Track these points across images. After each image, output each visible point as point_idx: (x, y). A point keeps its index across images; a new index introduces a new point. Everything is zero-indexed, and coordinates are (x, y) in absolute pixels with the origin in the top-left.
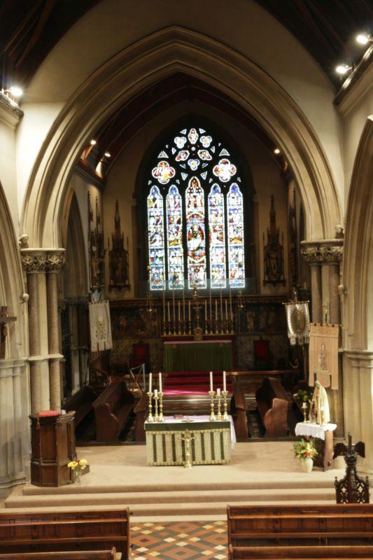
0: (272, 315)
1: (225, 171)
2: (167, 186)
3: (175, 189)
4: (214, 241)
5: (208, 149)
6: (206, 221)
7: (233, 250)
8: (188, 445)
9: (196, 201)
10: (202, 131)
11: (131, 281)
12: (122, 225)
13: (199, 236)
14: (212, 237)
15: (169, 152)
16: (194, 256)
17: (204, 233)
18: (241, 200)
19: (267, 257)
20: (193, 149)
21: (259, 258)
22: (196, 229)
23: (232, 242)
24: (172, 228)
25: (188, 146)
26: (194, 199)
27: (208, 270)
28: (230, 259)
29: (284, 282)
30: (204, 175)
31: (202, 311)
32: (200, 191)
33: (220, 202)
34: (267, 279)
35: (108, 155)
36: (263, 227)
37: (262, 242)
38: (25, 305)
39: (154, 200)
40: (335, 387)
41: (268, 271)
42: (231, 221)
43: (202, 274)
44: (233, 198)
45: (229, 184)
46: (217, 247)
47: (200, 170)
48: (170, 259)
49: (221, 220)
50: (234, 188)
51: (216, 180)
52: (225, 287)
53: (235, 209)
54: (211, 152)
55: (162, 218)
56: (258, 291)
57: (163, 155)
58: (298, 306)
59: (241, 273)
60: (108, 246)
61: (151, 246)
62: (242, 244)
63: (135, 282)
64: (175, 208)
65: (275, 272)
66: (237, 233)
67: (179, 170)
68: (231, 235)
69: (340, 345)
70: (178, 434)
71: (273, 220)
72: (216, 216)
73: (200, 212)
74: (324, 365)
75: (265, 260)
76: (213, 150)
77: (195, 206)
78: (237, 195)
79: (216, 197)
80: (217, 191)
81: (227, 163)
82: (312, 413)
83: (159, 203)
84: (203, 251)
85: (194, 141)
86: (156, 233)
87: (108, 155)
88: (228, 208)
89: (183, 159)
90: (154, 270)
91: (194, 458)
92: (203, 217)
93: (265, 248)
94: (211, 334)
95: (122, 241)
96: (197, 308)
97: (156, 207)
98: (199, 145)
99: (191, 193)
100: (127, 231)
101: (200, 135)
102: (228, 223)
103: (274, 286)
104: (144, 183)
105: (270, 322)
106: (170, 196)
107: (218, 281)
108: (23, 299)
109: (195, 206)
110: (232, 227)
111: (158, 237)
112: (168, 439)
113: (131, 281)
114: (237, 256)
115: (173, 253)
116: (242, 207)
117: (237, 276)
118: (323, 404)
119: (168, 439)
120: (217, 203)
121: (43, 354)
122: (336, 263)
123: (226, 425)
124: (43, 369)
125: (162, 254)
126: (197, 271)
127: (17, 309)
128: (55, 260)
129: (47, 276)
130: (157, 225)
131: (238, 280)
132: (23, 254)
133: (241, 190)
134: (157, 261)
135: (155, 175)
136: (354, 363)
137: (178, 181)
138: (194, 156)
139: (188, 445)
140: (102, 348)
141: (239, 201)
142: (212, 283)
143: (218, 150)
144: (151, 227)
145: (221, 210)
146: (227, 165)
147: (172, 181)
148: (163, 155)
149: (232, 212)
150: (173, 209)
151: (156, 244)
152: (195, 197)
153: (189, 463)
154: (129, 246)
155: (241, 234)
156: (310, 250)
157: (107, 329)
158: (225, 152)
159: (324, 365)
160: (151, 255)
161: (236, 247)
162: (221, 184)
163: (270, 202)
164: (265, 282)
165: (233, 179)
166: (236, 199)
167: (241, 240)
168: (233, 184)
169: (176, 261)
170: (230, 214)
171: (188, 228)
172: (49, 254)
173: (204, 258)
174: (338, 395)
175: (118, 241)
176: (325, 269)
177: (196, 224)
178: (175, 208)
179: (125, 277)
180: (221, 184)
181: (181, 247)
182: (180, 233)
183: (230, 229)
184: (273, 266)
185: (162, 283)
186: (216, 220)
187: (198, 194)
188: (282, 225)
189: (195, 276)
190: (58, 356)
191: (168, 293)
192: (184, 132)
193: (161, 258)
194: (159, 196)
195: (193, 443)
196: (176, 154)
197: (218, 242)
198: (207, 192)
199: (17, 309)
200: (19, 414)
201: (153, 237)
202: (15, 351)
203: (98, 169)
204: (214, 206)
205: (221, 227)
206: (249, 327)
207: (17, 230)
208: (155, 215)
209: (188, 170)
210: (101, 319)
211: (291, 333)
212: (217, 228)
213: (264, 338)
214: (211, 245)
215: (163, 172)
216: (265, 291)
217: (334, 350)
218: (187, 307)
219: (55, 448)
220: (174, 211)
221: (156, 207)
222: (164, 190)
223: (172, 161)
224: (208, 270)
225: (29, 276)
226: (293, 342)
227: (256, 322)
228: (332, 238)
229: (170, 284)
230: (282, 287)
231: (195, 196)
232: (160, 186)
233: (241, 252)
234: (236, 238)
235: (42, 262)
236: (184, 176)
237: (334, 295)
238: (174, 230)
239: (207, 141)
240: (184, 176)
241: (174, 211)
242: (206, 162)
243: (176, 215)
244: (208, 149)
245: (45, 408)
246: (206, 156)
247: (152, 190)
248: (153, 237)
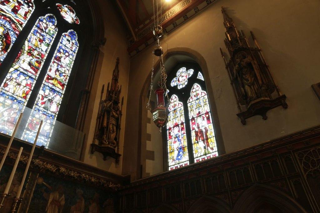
6: (23, 36)
7: (47, 92)
14: (22, 58)
17: (12, 45)
18: (76, 48)
21: (92, 111)
23: (51, 81)
28: (39, 101)
29: (116, 156)
32: (31, 5)
33: (52, 32)
34: (97, 143)
41: (101, 131)
42: (59, 59)
44: (68, 40)
46: (24, 74)
53: (67, 52)
56: (82, 157)
66: (60, 75)
68: (51, 73)
71: (115, 79)
72: (41, 41)
73: (19, 21)
77: (15, 11)
78: (74, 41)
80: (53, 22)
81: (73, 13)
88: (59, 45)
93: (101, 103)
102: (53, 58)
103: (105, 159)
109: (15, 11)
110: (56, 65)
114: (51, 101)
116: (75, 55)
120: (47, 31)
133: (77, 40)
141: (74, 48)
146: (72, 14)
149: (62, 51)
155: (65, 79)
161: (52, 90)
164: (93, 145)
167: (63, 85)
168: (72, 30)
170: (60, 52)
183: (53, 66)
184: (111, 126)
187: (26, 6)
197: (28, 68)
204: (42, 30)
205: (42, 56)
212: (35, 53)
230: (113, 164)
233: (58, 99)
234: (56, 79)
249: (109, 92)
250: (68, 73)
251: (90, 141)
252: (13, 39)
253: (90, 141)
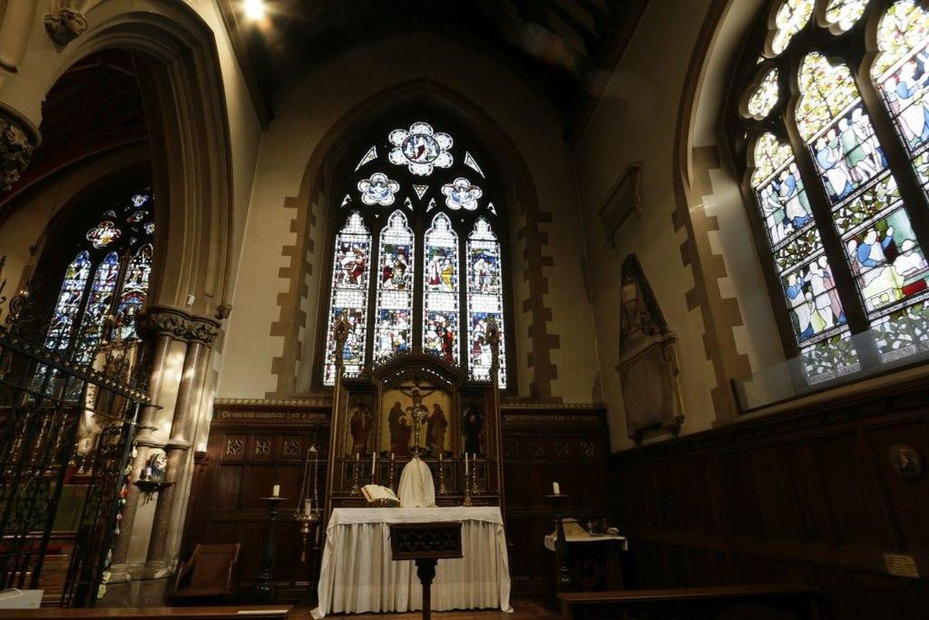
3: (114, 257)
9: (142, 275)
22: (131, 311)
26: (140, 272)
39: (78, 269)
64: (107, 281)
83: (84, 273)
86: (67, 314)
97: (78, 278)
99: (138, 263)
109: (139, 281)
130: (71, 302)
135: (91, 237)
144: (61, 308)
148: (113, 213)
150: (103, 283)
152: (142, 269)
178: (107, 281)
201: (59, 319)
208: (73, 288)
220: (104, 286)
221: (78, 278)
223: (118, 223)
241: (104, 286)
243: (106, 290)
248: (59, 319)
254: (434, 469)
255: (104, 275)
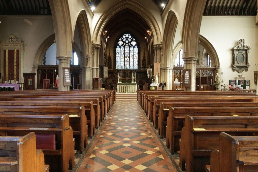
0: (143, 75)
1: (134, 43)
2: (121, 46)
4: (131, 58)
5: (130, 38)
6: (129, 54)
8: (127, 88)
10: (129, 34)
11: (112, 66)
12: (111, 54)
13: (128, 57)
15: (122, 39)
16: (126, 62)
18: (137, 50)
19: (143, 62)
20: (127, 38)
22: (127, 56)
24: (122, 55)
25: (126, 38)
27: (129, 65)
30: (129, 44)
31: (128, 73)
35: (108, 37)
36: (142, 55)
37: (142, 59)
38: (92, 56)
39: (118, 49)
40: (159, 76)
41: (143, 65)
42: (135, 54)
43: (128, 66)
45: (135, 46)
47: (128, 43)
48: (121, 62)
49: (133, 54)
50: (136, 47)
51: (132, 45)
52: (133, 69)
54: (131, 39)
55: (120, 53)
56: (141, 70)
57: (120, 39)
58: (150, 69)
59: (137, 66)
60: (107, 56)
61: (117, 59)
62: (137, 59)
63: (113, 66)
65: (144, 65)
67: (124, 43)
68: (135, 57)
69: (161, 67)
70: (124, 86)
74: (157, 71)
75: (142, 63)
76: (131, 39)
79: (132, 49)
82: (154, 81)
83: (119, 50)
84: (128, 61)
85: (127, 36)
87: (108, 37)
88: (134, 51)
89: (125, 40)
90: (117, 65)
91: (128, 91)
92: (129, 53)
93: (142, 60)
94: (130, 78)
95: (111, 57)
96: (127, 73)
98: (128, 38)
100: (112, 55)
101: (129, 35)
104: (116, 45)
105: (143, 76)
106: (121, 48)
107: (131, 68)
108: (92, 54)
111: (118, 57)
112: (122, 87)
113: (112, 66)
115: (122, 61)
117: (136, 66)
118: (157, 79)
119: (122, 87)
121: (95, 67)
122: (160, 49)
123: (135, 84)
124: (95, 70)
125: (119, 61)
126: (127, 65)
127: (90, 56)
128: (99, 46)
129: (97, 50)
131: (136, 67)
132: (92, 44)
134: (118, 63)
136: (164, 70)
137: (123, 45)
138: (127, 40)
139: (127, 88)
140: (106, 77)
142: (130, 68)
143: (133, 39)
144: (117, 55)
145: (133, 52)
147: (122, 45)
150: (122, 51)
151: (118, 59)
153: (127, 92)
154: (112, 59)
155: (137, 57)
156: (155, 46)
157: (107, 73)
158: (134, 39)
159: (157, 71)
160: (117, 61)
162: (133, 46)
163: (144, 50)
164: (142, 68)
165: (136, 45)
166: (136, 49)
169: (122, 62)
171: (125, 56)
172: (98, 45)
173: (129, 62)
174: (160, 77)
175: (110, 57)
176: (158, 51)
177: (127, 55)
179: (111, 65)
180: (133, 46)
181: (123, 59)
182: (123, 57)
183: (135, 56)
185: (119, 67)
186: (131, 54)
188: (146, 55)
189: (126, 66)
190: (98, 67)
191: (120, 69)
192: (125, 34)
193: (119, 62)
194: (119, 48)
195: (128, 88)
196: (123, 39)
197: (132, 59)
198: (130, 48)
199: (90, 56)
200: (90, 79)
202: (89, 65)
203: (106, 40)
206: (138, 77)
207: (91, 39)
209: (126, 43)
210: (106, 71)
211: (148, 75)
213: (141, 80)
214: (130, 59)
215: (120, 43)
216: (142, 70)
217: (159, 67)
218: (124, 72)
219: (98, 85)
222: (120, 47)
223: (122, 41)
224: (129, 65)
225: (93, 49)
226: (148, 77)
227: (140, 76)
228: (160, 43)
229: (121, 68)
231: (127, 48)
232: (119, 46)
235: (96, 46)
236: (125, 44)
237: (160, 56)
238: (122, 56)
239: (130, 37)
240: (125, 44)
242: (130, 41)
243: (123, 52)
244: (130, 38)
245: (95, 77)
246: (130, 40)
247: (118, 47)
249: (143, 58)
250: (137, 56)
251: (141, 67)
252: (129, 56)
253: (141, 67)
254: (178, 79)
255: (122, 50)
